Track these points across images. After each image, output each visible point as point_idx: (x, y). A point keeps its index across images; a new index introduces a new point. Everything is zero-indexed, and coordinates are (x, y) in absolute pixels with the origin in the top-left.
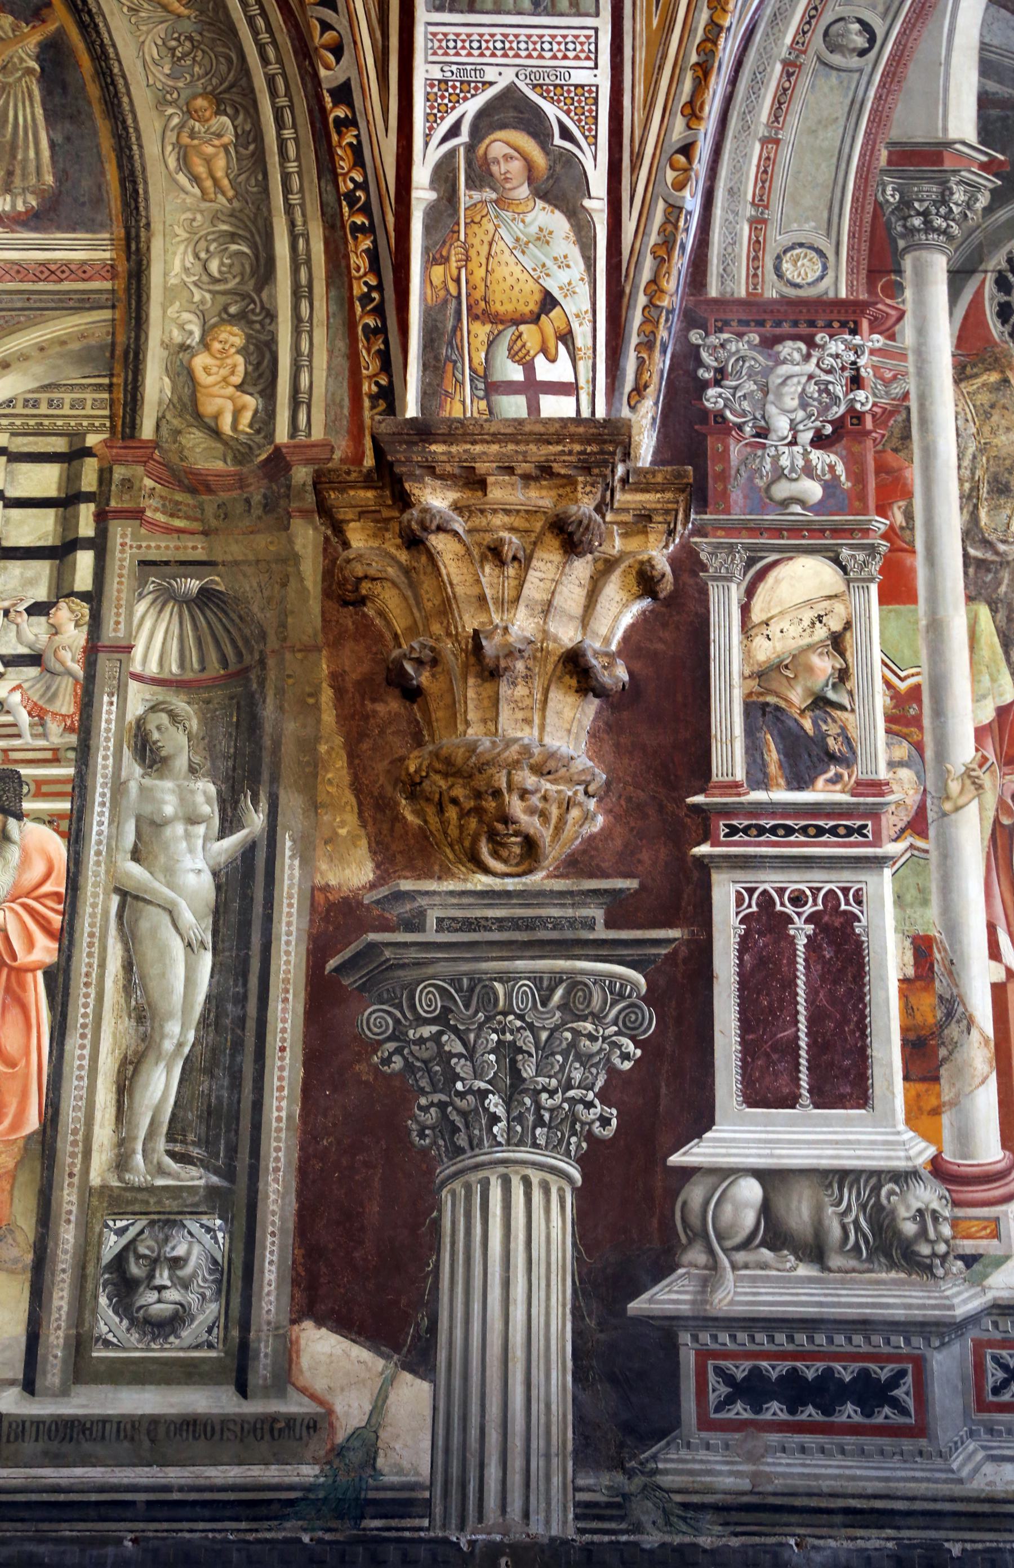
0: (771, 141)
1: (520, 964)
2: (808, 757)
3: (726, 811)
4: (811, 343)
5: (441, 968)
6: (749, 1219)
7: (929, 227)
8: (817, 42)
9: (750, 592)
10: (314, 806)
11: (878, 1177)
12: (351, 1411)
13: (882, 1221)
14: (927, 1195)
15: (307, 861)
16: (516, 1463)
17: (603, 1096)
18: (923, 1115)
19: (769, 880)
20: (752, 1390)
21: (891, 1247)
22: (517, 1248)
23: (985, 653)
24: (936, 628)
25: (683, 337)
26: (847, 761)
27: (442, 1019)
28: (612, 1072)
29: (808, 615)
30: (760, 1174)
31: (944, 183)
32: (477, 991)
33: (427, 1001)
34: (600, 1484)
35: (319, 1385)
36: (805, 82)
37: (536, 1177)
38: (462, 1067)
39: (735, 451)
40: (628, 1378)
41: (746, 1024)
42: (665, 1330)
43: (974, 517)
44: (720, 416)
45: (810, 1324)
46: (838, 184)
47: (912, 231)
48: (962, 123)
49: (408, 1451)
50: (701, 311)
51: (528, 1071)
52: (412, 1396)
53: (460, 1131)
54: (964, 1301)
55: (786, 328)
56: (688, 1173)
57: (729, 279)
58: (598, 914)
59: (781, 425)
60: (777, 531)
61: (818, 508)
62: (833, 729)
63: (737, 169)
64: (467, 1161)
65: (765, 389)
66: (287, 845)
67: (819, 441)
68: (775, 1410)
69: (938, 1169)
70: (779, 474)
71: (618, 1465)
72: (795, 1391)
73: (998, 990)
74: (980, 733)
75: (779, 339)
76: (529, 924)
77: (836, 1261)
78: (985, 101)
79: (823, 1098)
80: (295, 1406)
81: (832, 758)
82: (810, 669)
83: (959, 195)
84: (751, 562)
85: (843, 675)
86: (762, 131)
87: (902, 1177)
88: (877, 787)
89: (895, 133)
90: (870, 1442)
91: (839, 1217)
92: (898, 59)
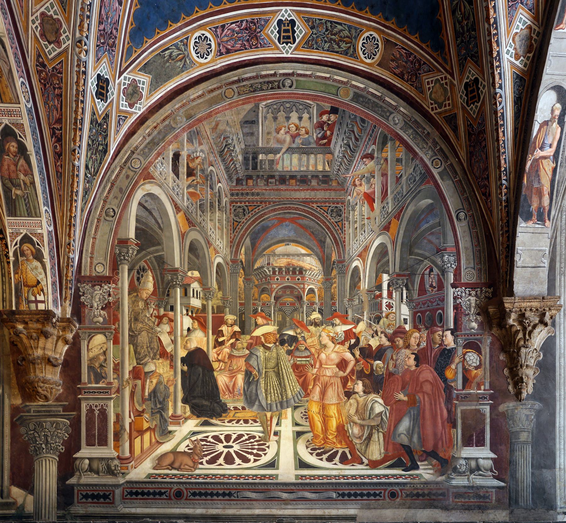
0: (94, 238)
1: (48, 419)
2: (99, 377)
3: (84, 389)
4: (101, 286)
5: (34, 420)
6: (87, 467)
7: (125, 259)
8: (104, 214)
9: (89, 342)
10: (10, 388)
11: (108, 459)
12: (20, 501)
13: (109, 467)
14: (116, 462)
15: (10, 399)
16: (47, 509)
17: (62, 445)
18: (116, 448)
19: (91, 403)
20: (86, 497)
21: (111, 472)
22: (48, 472)
23: (131, 355)
24: (123, 350)
25: (76, 285)
26: (106, 378)
27: (34, 430)
28: (64, 440)
29: (99, 347)
30: (89, 459)
31: (128, 248)
32: (40, 425)
33: (32, 426)
34: (61, 513)
35: (15, 497)
36: (101, 223)
37: (51, 459)
38: (38, 439)
39: (86, 311)
40: (66, 494)
41: (87, 430)
42: (72, 486)
43: (131, 325)
44: (83, 303)
45: (96, 485)
46: (107, 249)
47: (121, 260)
48: (132, 234)
49: (30, 508)
50: (80, 278)
51: (49, 440)
52: (30, 498)
53: (38, 451)
54: (122, 481)
55: (97, 283)
56: (76, 458)
57: (85, 272)
58: (61, 409)
59: (95, 305)
60: (94, 329)
61: (102, 324)
62: (103, 371)
63: (88, 245)
64: (39, 457)
65: (92, 297)
66: (6, 396)
67: (103, 309)
68: (90, 500)
69: (119, 457)
70: (95, 316)
71: (64, 509)
72: (93, 497)
73: (130, 424)
74: (130, 372)
75: (95, 285)
76: (49, 411)
77: (101, 474)
78: (137, 229)
79: (100, 444)
80: (11, 500)
81: (103, 377)
82: (99, 359)
83: (131, 252)
84: (89, 336)
85: (105, 360)
86: (93, 236)
87: (112, 459)
88: (111, 383)
89: (119, 236)
90: (105, 505)
91: (102, 466)
92: (120, 218)
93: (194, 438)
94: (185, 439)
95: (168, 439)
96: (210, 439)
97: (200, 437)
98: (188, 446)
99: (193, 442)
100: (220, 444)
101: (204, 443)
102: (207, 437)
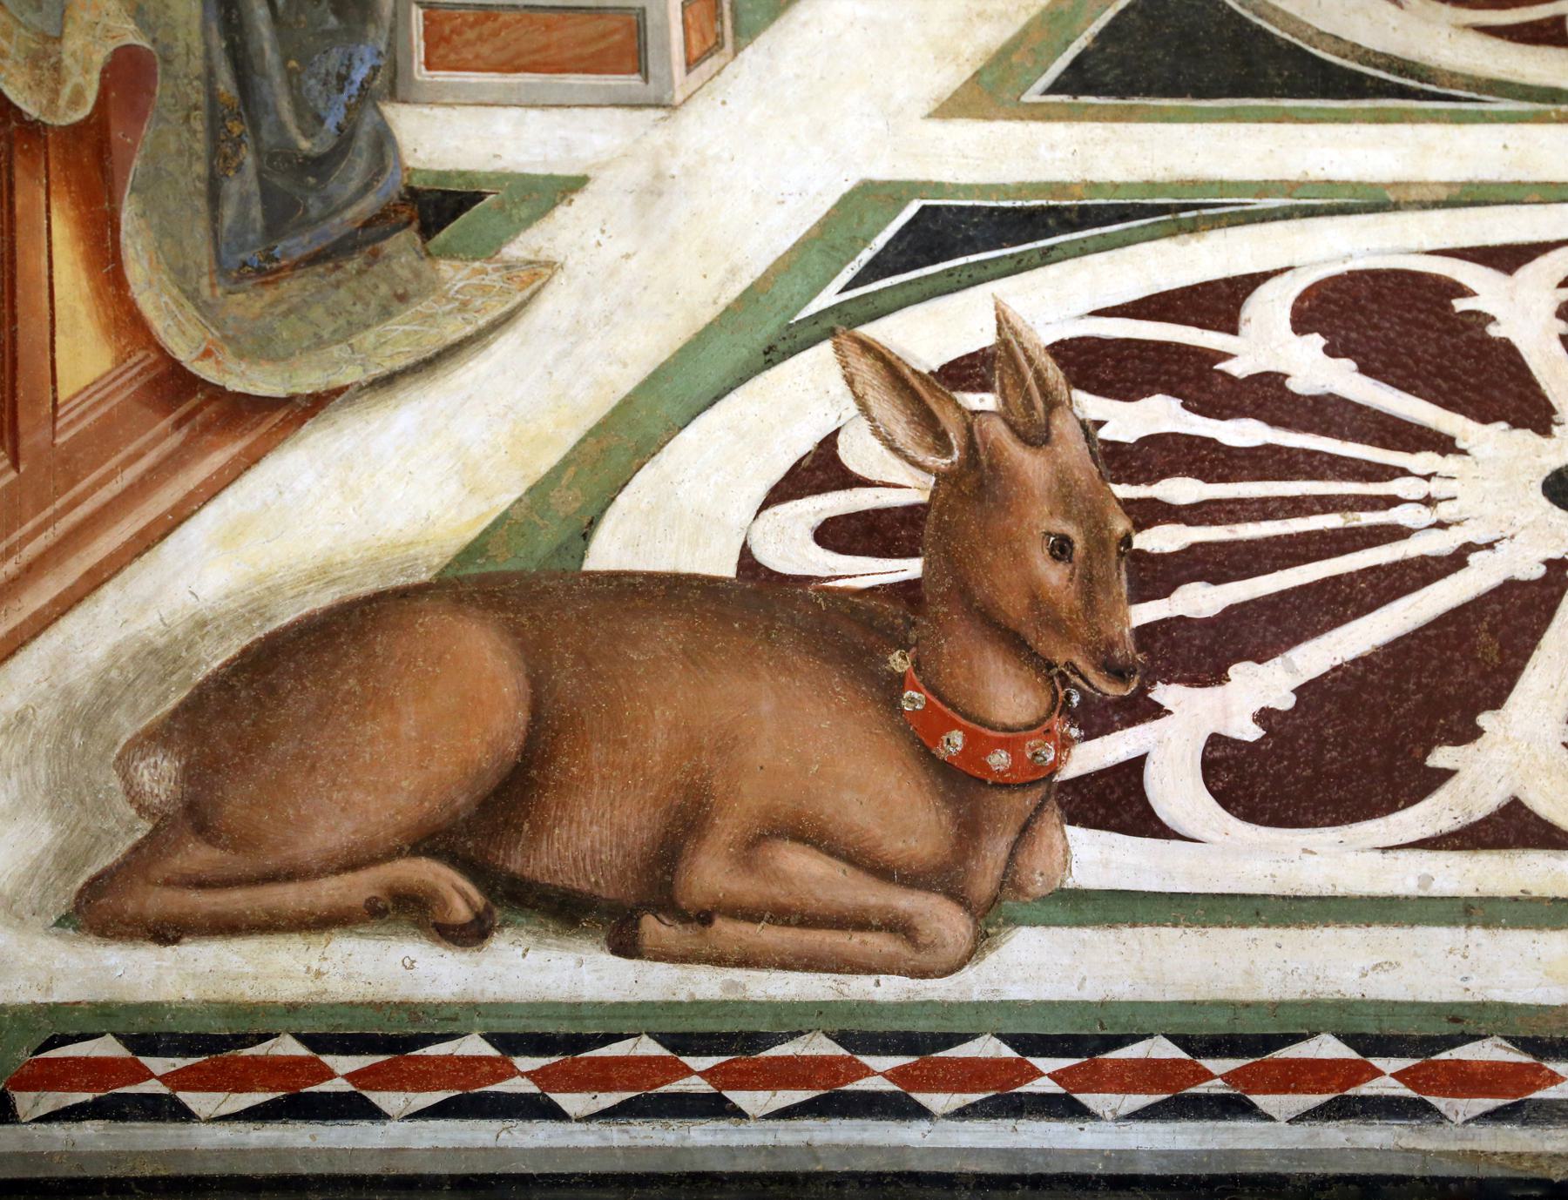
93: (932, 333)
94: (754, 336)
95: (399, 339)
96: (1266, 342)
97: (1060, 300)
98: (821, 469)
99: (919, 395)
100: (1490, 442)
101: (1162, 414)
102: (1220, 302)
